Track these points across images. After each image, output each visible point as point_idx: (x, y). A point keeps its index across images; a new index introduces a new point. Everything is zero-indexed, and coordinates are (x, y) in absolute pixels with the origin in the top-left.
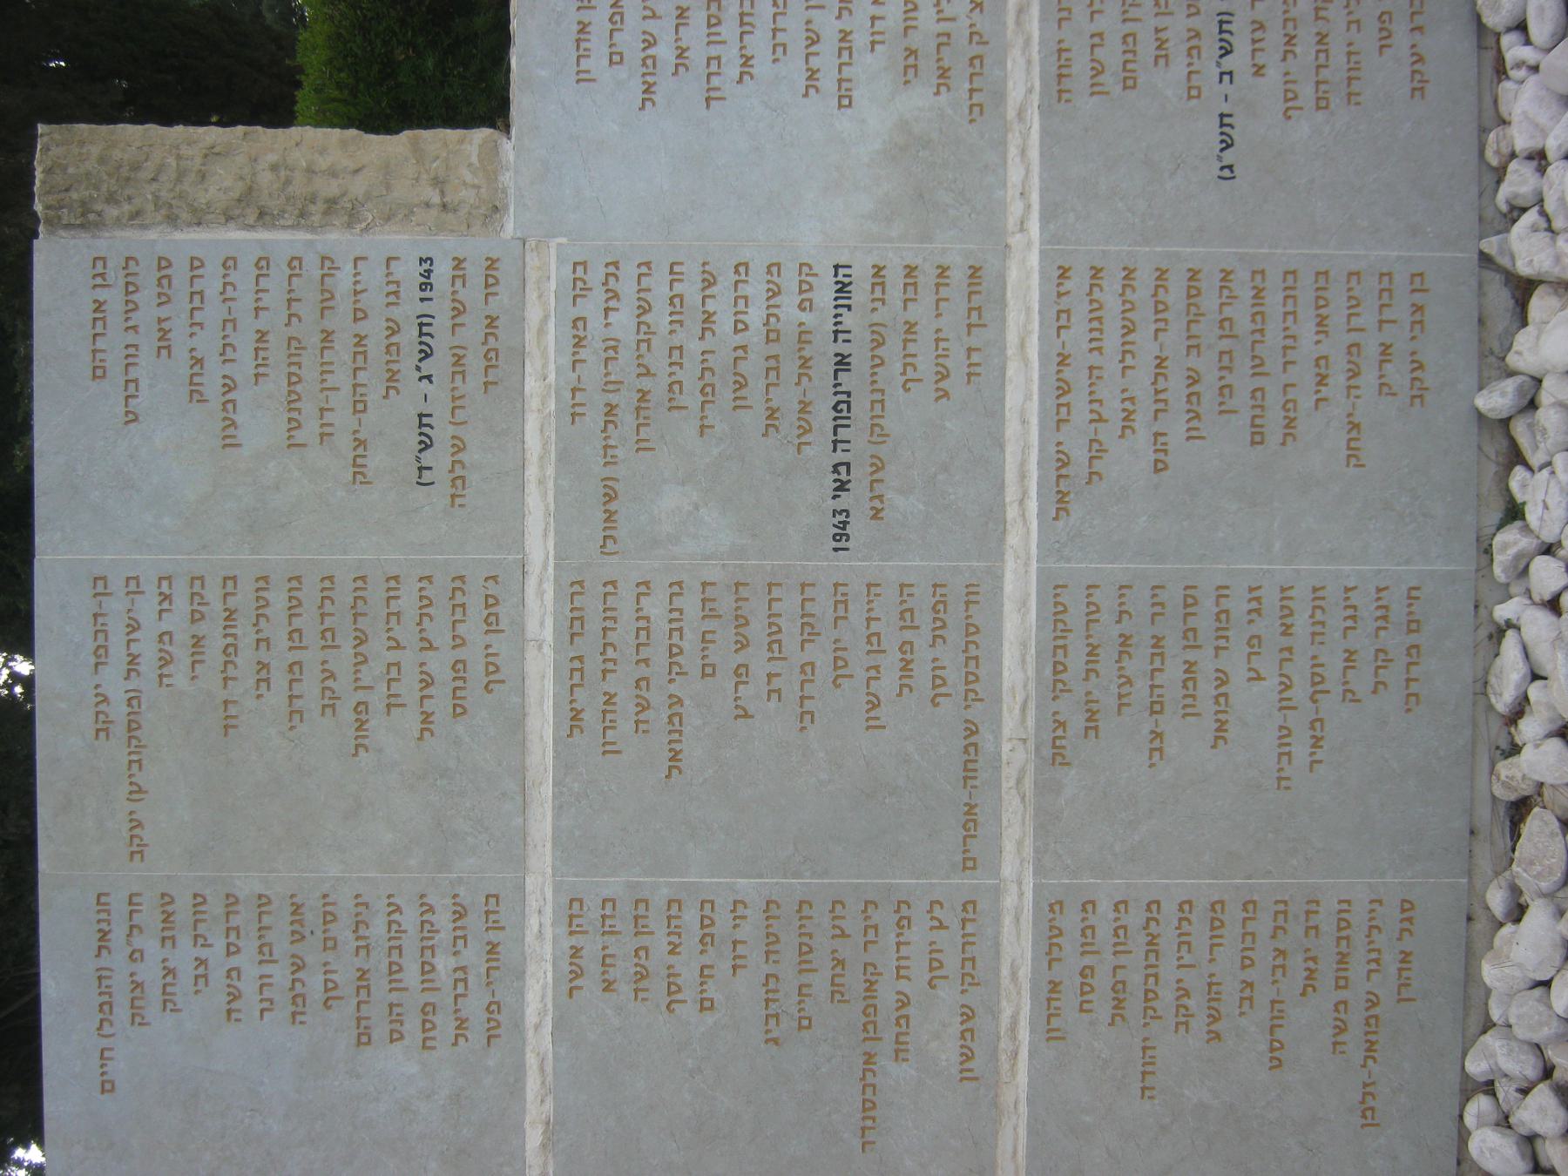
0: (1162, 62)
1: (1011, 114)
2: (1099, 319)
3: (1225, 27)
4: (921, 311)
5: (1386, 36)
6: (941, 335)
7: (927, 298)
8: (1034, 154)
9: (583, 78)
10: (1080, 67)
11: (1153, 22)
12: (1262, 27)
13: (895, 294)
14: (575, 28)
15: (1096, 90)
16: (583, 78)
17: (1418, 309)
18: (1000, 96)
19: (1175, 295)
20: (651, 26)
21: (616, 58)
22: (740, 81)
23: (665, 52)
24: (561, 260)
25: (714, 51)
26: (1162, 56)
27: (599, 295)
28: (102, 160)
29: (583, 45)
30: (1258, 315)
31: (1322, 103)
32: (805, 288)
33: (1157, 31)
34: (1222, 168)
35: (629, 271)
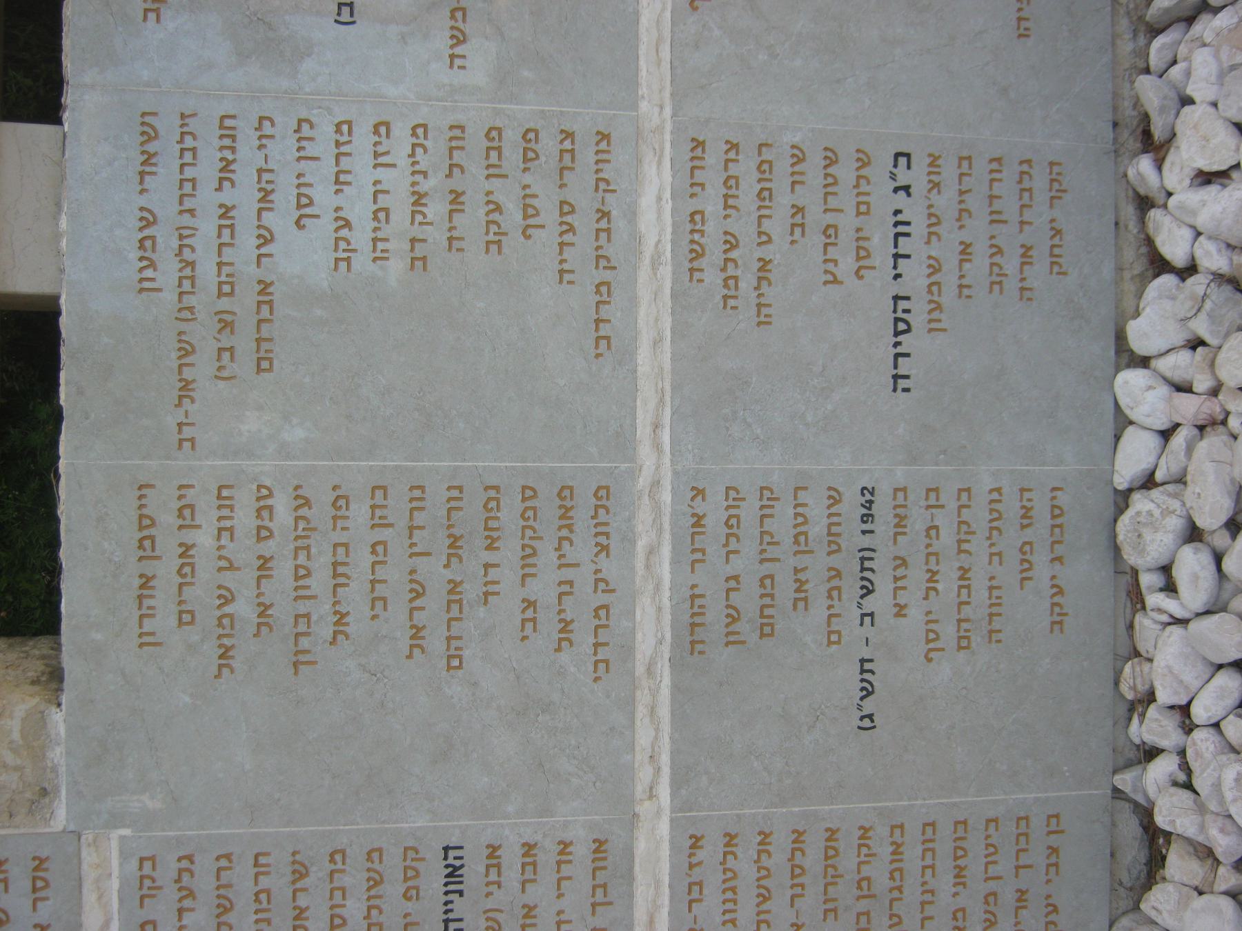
0: (801, 605)
1: (640, 670)
2: (733, 889)
3: (867, 564)
4: (540, 893)
5: (1026, 566)
6: (563, 917)
7: (547, 876)
8: (664, 712)
9: (147, 641)
10: (715, 614)
11: (793, 562)
12: (904, 563)
13: (512, 875)
14: (137, 582)
15: (732, 639)
16: (147, 641)
17: (1054, 850)
18: (629, 650)
19: (812, 858)
20: (228, 579)
21: (186, 617)
22: (334, 642)
23: (244, 608)
24: (124, 856)
25: (302, 608)
26: (801, 600)
27: (170, 894)
29: (146, 602)
30: (896, 872)
31: (963, 643)
32: (411, 873)
33: (796, 571)
34: (862, 718)
35: (205, 866)
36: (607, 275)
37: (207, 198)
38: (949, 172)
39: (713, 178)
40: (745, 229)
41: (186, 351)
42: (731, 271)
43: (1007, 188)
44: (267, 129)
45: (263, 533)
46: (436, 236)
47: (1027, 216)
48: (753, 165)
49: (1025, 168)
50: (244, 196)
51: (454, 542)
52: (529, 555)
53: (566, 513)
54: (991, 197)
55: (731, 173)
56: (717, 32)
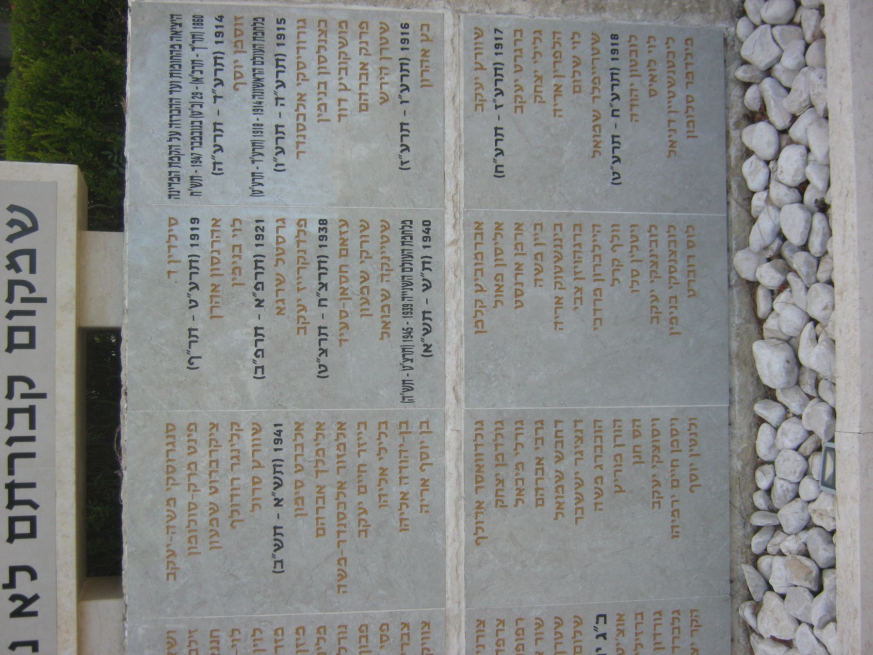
38: (629, 623)
43: (665, 629)
44: (237, 636)
47: (677, 643)
48: (513, 631)
49: (676, 615)
54: (655, 635)
55: (500, 637)
56: (491, 557)
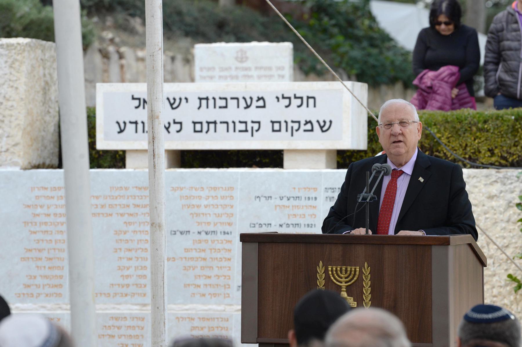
9: (33, 189)
16: (33, 189)
20: (46, 207)
21: (37, 197)
22: (30, 231)
23: (39, 210)
25: (38, 224)
28: (16, 60)
36: (112, 295)
37: (131, 201)
39: (134, 323)
40: (123, 331)
41: (97, 197)
42: (112, 328)
45: (55, 215)
46: (122, 254)
50: (132, 210)
51: (51, 259)
52: (46, 277)
53: (56, 286)
